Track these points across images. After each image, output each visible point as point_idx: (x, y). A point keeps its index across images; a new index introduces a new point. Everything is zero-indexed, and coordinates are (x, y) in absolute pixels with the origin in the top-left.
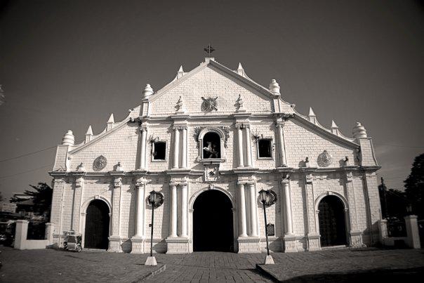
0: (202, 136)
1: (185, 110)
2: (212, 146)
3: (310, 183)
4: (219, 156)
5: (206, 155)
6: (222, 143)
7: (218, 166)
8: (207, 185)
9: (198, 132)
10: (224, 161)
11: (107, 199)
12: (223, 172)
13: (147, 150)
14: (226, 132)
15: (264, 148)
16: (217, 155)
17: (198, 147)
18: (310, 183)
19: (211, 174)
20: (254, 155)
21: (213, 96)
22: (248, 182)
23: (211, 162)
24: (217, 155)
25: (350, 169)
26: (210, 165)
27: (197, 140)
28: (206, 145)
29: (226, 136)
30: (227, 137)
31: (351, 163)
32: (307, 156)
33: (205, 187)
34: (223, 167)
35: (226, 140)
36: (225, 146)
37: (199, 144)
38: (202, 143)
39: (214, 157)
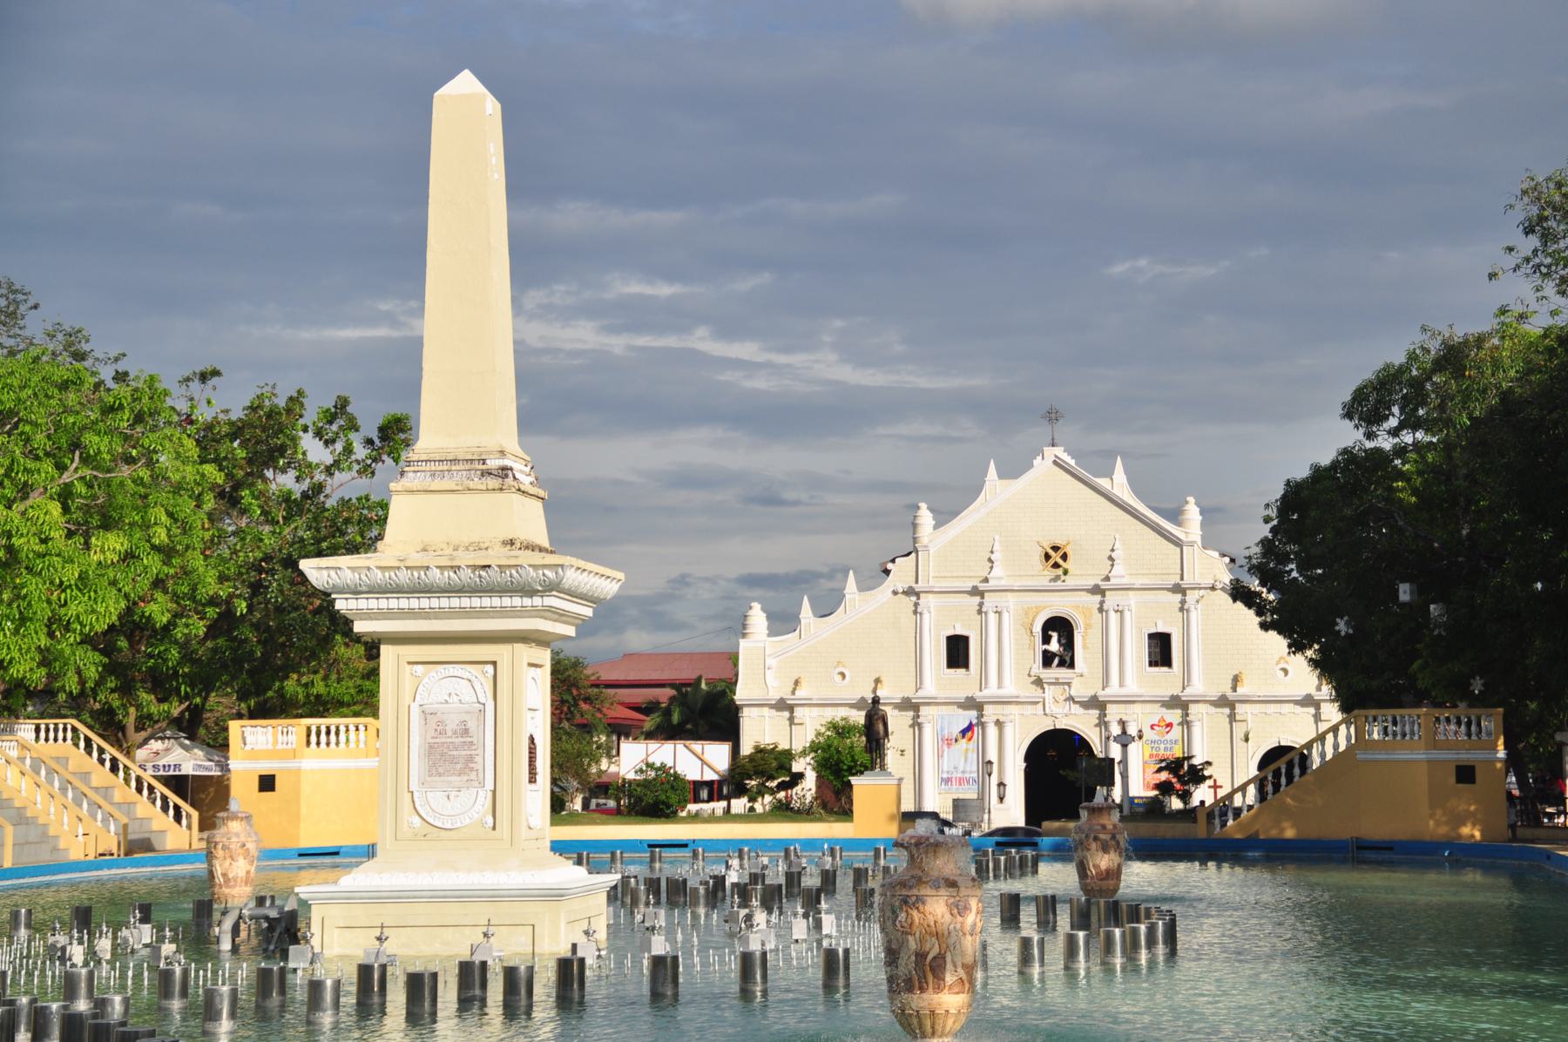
0: (1038, 628)
2: (1059, 641)
4: (1072, 665)
5: (1048, 659)
7: (1069, 684)
13: (936, 652)
28: (1046, 640)
30: (1088, 626)
33: (1046, 725)
34: (1081, 690)
39: (1062, 664)
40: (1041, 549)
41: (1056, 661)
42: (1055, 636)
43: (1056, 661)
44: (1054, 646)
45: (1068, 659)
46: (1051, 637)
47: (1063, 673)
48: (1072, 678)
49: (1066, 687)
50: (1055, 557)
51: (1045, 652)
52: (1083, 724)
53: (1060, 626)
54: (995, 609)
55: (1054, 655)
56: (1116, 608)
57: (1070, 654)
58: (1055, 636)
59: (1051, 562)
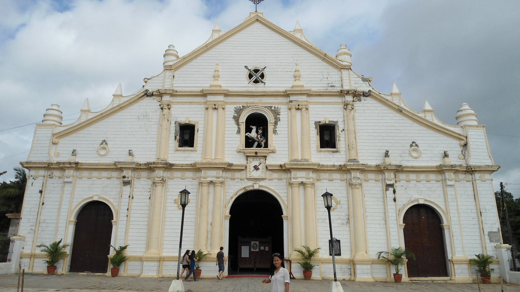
0: (243, 119)
1: (225, 84)
2: (257, 132)
4: (266, 146)
5: (249, 142)
6: (270, 128)
8: (250, 183)
9: (239, 111)
10: (273, 152)
11: (111, 200)
12: (271, 166)
14: (276, 113)
16: (263, 144)
17: (239, 132)
18: (392, 185)
19: (256, 168)
20: (315, 149)
21: (260, 67)
22: (304, 180)
23: (256, 153)
24: (263, 144)
25: (454, 169)
26: (256, 156)
27: (238, 124)
28: (248, 130)
29: (276, 118)
31: (454, 160)
32: (387, 149)
34: (273, 160)
35: (276, 123)
36: (275, 132)
37: (239, 128)
39: (259, 146)
40: (247, 71)
41: (256, 143)
42: (254, 129)
43: (256, 143)
44: (253, 134)
46: (252, 129)
47: (261, 151)
48: (266, 153)
49: (262, 160)
51: (247, 138)
54: (214, 107)
55: (254, 141)
56: (297, 107)
57: (264, 141)
58: (254, 129)
59: (254, 78)
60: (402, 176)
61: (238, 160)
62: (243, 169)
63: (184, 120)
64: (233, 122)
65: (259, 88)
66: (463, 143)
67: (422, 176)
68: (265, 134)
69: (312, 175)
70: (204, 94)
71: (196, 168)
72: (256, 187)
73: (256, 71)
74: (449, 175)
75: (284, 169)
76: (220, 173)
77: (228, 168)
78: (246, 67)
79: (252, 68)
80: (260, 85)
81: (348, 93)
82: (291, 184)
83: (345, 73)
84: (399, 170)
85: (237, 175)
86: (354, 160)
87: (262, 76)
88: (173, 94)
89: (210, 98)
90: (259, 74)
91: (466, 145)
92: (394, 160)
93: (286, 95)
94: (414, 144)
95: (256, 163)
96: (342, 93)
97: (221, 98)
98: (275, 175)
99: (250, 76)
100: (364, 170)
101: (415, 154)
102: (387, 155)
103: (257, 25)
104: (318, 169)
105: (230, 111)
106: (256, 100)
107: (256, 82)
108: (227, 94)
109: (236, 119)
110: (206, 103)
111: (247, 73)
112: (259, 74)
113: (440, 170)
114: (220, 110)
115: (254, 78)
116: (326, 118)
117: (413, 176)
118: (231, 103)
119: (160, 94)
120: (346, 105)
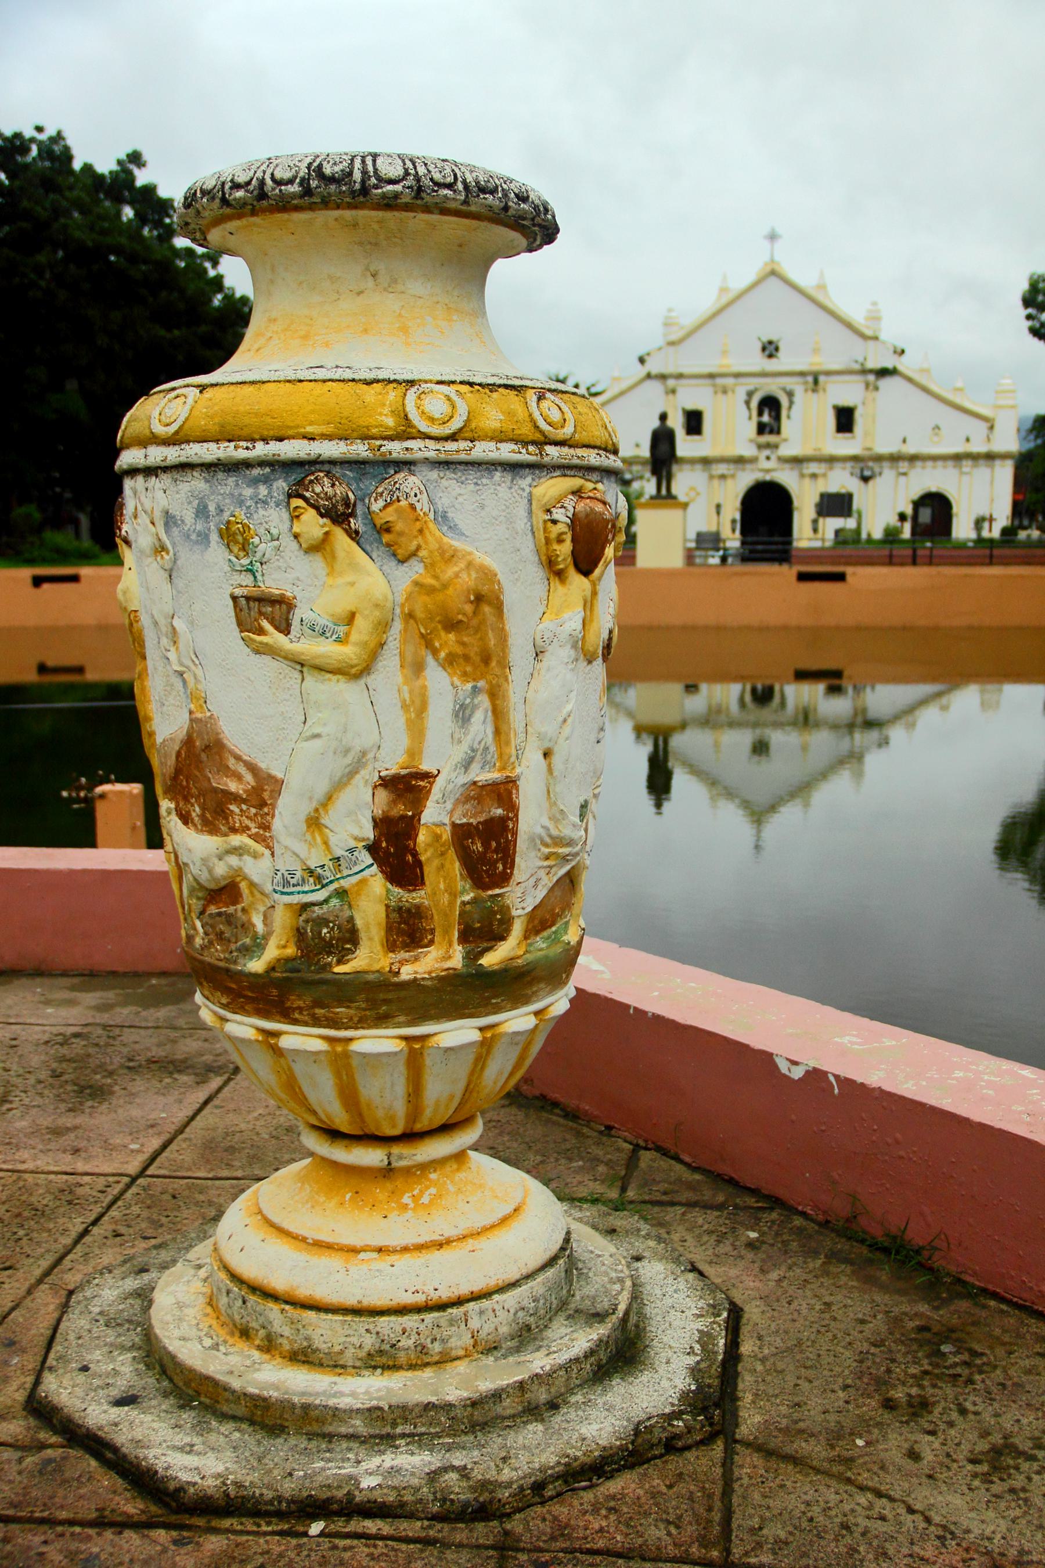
0: (754, 404)
2: (770, 415)
3: (905, 474)
4: (778, 432)
5: (761, 429)
6: (784, 413)
9: (750, 394)
10: (785, 440)
14: (790, 394)
15: (845, 420)
17: (750, 418)
19: (768, 458)
21: (774, 338)
26: (768, 446)
27: (749, 408)
28: (760, 413)
30: (791, 403)
35: (790, 407)
36: (789, 417)
38: (755, 413)
39: (771, 432)
43: (768, 430)
44: (766, 418)
45: (776, 428)
50: (770, 349)
52: (786, 478)
53: (770, 404)
59: (767, 353)
60: (919, 464)
61: (748, 451)
62: (753, 460)
63: (690, 406)
64: (744, 407)
65: (772, 365)
66: (989, 425)
67: (940, 463)
68: (777, 418)
69: (823, 465)
70: (711, 376)
71: (706, 462)
72: (768, 478)
73: (770, 343)
74: (967, 464)
75: (797, 461)
76: (732, 466)
77: (740, 461)
78: (759, 339)
79: (765, 339)
80: (774, 360)
81: (871, 371)
82: (802, 476)
83: (871, 343)
84: (913, 458)
85: (748, 466)
86: (869, 449)
87: (777, 349)
88: (680, 376)
89: (719, 381)
90: (772, 347)
91: (991, 428)
92: (910, 449)
93: (802, 374)
94: (937, 427)
95: (767, 452)
96: (864, 372)
97: (729, 381)
98: (787, 466)
99: (764, 349)
100: (879, 458)
101: (936, 439)
102: (904, 441)
103: (773, 281)
104: (831, 460)
105: (741, 394)
106: (768, 380)
107: (770, 356)
108: (737, 375)
109: (748, 403)
110: (714, 386)
111: (759, 346)
112: (772, 347)
113: (958, 458)
114: (730, 393)
115: (767, 353)
116: (845, 402)
117: (929, 464)
118: (742, 384)
119: (663, 377)
120: (867, 385)
